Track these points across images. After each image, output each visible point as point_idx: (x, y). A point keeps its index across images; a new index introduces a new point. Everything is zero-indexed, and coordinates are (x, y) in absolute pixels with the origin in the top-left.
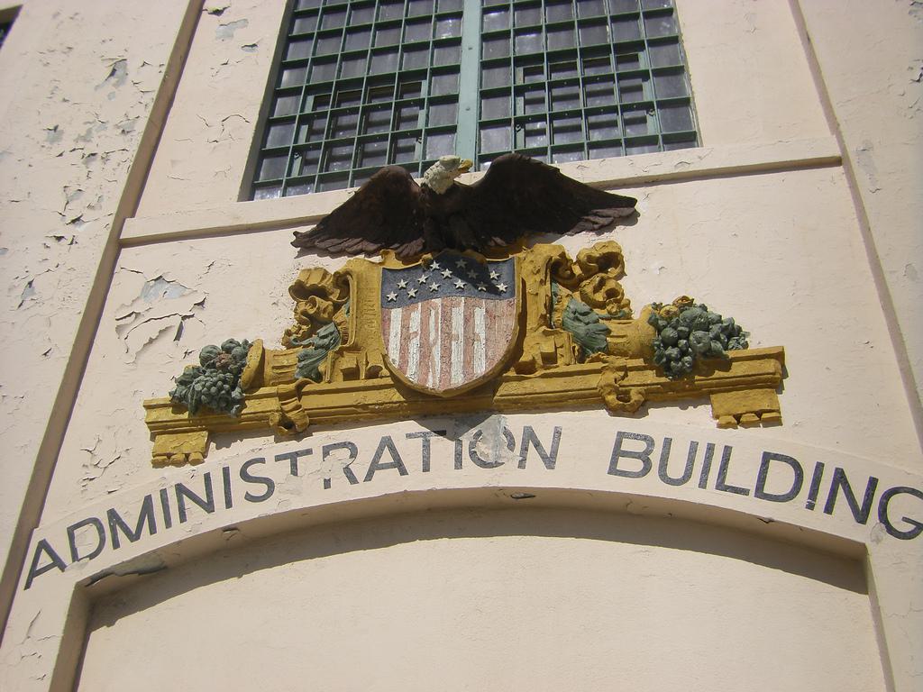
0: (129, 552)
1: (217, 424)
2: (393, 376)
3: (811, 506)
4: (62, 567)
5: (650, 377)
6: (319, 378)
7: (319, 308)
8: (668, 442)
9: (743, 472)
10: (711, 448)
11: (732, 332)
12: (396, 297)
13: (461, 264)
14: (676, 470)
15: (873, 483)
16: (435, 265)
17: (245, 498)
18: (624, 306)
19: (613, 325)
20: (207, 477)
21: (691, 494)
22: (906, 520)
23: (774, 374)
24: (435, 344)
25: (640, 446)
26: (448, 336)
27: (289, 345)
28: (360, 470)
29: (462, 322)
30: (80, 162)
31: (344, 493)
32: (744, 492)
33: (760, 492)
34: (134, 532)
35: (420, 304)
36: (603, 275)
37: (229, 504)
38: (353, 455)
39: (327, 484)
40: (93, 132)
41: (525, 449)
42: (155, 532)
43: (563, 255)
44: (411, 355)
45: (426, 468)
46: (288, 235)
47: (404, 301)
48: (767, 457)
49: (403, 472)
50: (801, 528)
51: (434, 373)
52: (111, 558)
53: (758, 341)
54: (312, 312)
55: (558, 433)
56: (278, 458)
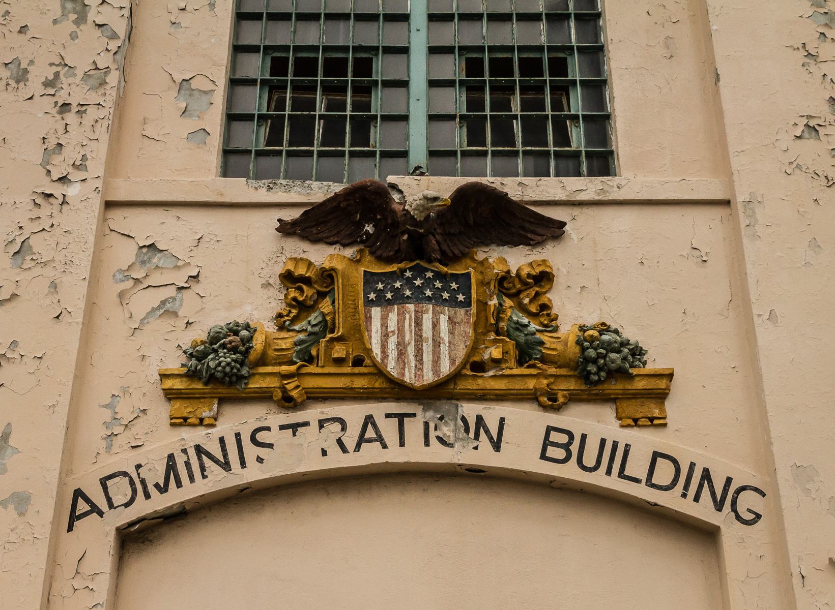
0: (160, 503)
1: (217, 389)
2: (375, 365)
3: (684, 496)
4: (101, 514)
5: (572, 385)
6: (310, 360)
7: (307, 296)
8: (584, 437)
9: (637, 466)
10: (615, 445)
11: (637, 352)
12: (375, 297)
13: (429, 275)
14: (589, 461)
15: (729, 481)
16: (408, 274)
17: (257, 460)
18: (552, 320)
19: (547, 338)
20: (222, 440)
21: (600, 479)
22: (749, 511)
23: (665, 389)
24: (409, 344)
25: (563, 439)
26: (419, 339)
27: (281, 328)
28: (350, 443)
29: (431, 327)
30: (54, 111)
31: (337, 461)
32: (637, 481)
33: (650, 483)
34: (162, 486)
35: (396, 306)
36: (538, 289)
37: (243, 464)
38: (344, 429)
39: (324, 453)
40: (62, 76)
41: (477, 437)
42: (181, 486)
43: (508, 272)
44: (389, 351)
45: (402, 444)
46: (271, 218)
47: (381, 301)
48: (656, 455)
49: (385, 446)
50: (676, 511)
51: (409, 368)
52: (143, 508)
53: (655, 362)
54: (301, 299)
55: (502, 420)
56: (282, 427)
